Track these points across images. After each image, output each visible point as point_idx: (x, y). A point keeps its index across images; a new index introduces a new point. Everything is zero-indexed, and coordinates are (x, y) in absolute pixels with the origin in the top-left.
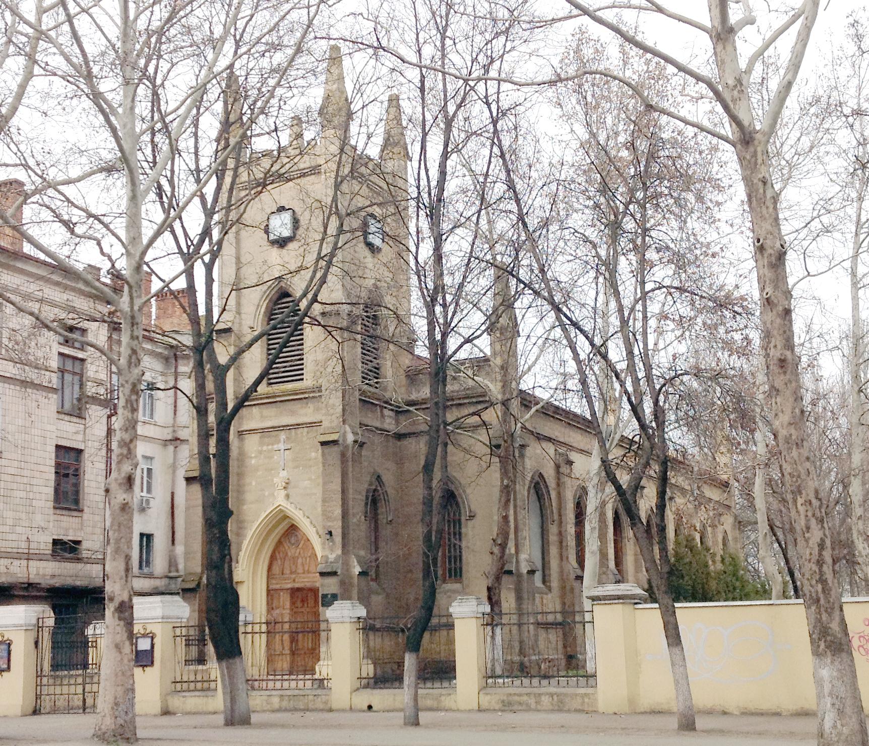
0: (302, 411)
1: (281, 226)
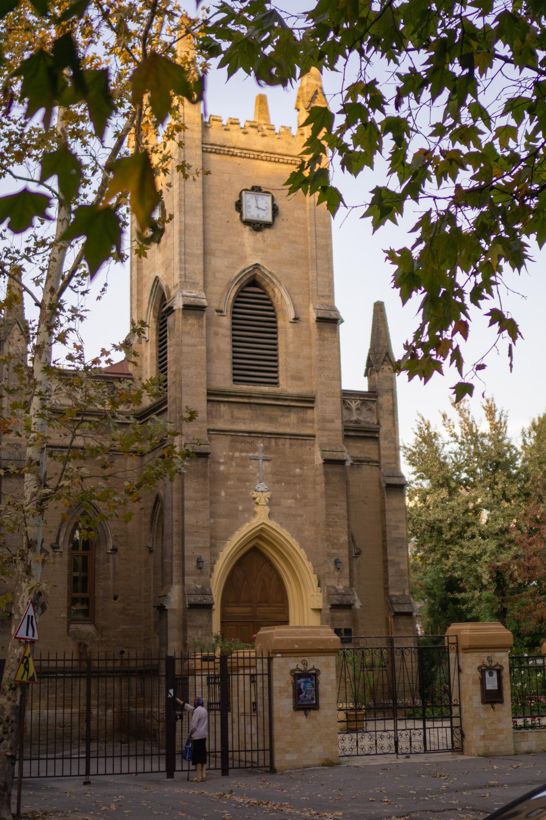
0: (282, 420)
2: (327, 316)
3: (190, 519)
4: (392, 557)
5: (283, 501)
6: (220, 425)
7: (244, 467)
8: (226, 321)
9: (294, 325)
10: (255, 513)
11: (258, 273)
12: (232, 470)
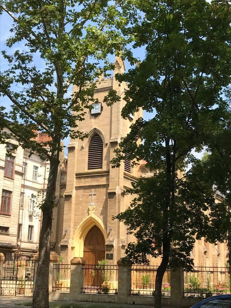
7: (87, 198)
11: (96, 131)
12: (84, 199)
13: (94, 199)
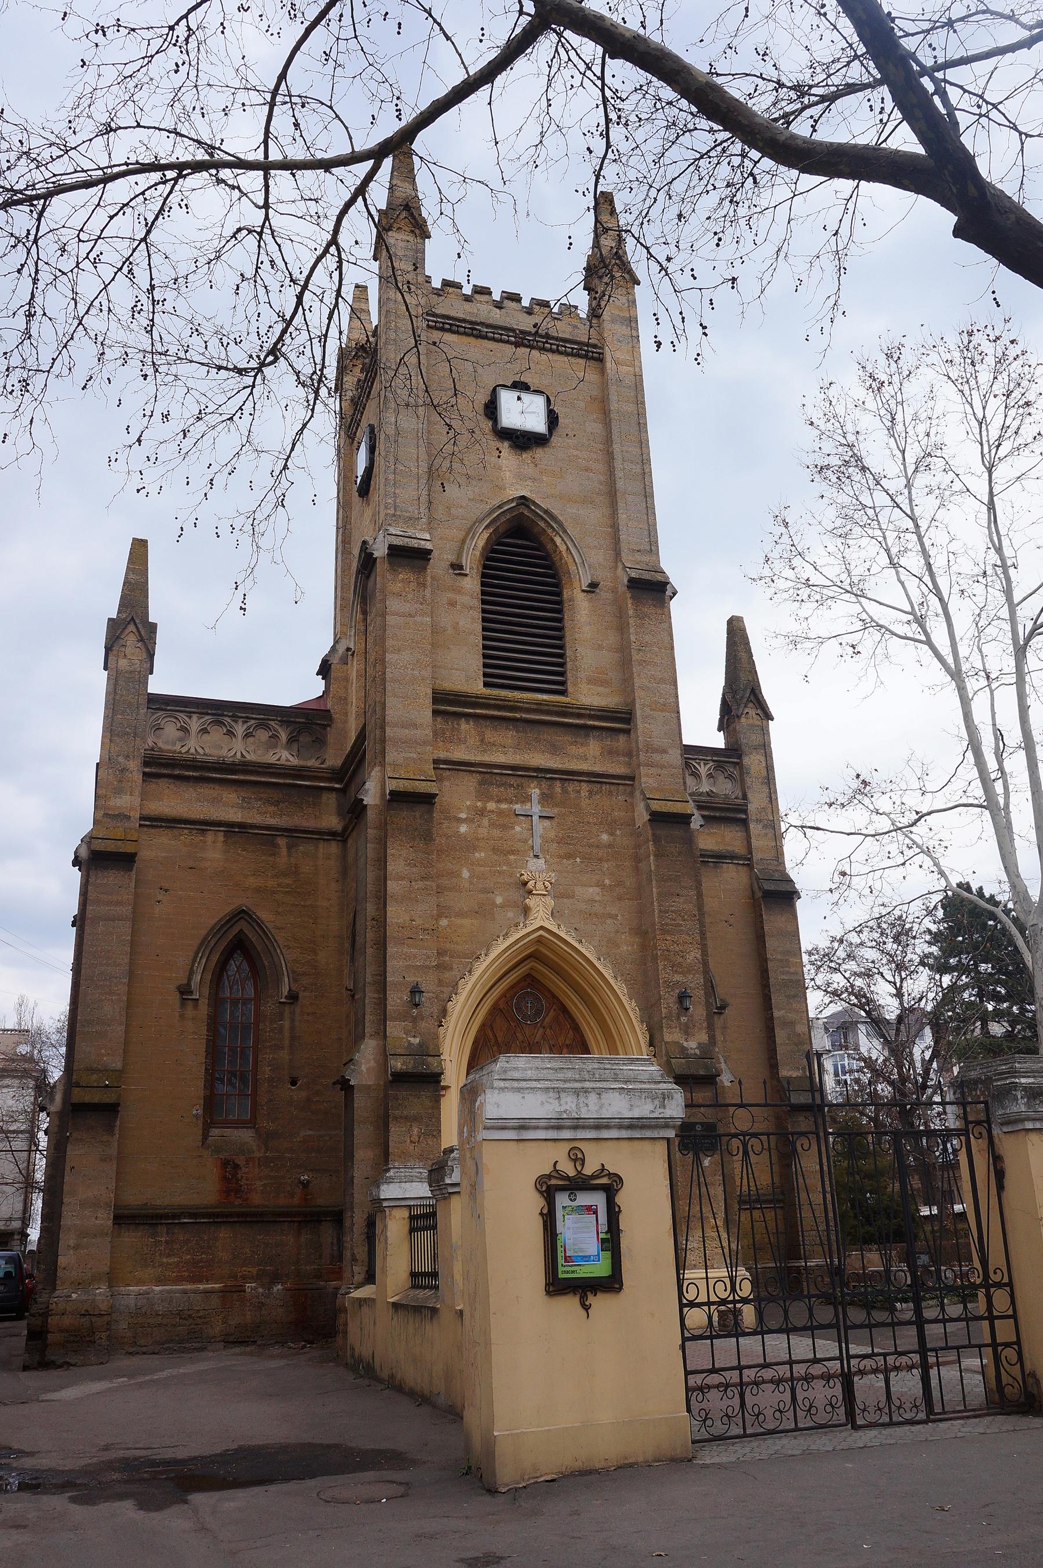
0: (573, 750)
1: (522, 412)
2: (647, 576)
3: (396, 914)
4: (782, 1012)
5: (579, 891)
6: (460, 754)
7: (505, 827)
8: (472, 584)
9: (590, 596)
10: (526, 910)
12: (483, 832)
13: (545, 840)
